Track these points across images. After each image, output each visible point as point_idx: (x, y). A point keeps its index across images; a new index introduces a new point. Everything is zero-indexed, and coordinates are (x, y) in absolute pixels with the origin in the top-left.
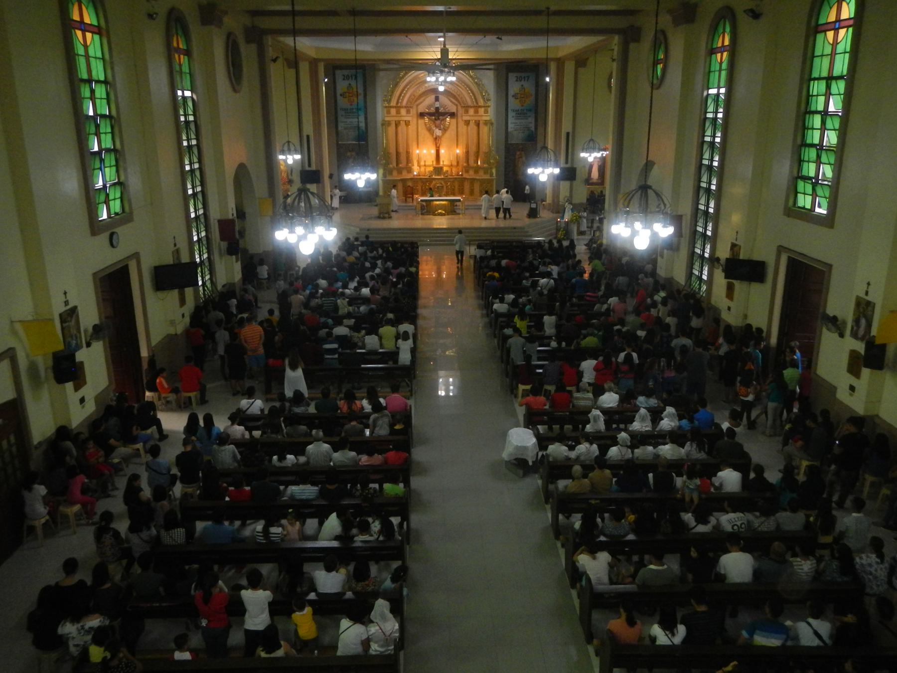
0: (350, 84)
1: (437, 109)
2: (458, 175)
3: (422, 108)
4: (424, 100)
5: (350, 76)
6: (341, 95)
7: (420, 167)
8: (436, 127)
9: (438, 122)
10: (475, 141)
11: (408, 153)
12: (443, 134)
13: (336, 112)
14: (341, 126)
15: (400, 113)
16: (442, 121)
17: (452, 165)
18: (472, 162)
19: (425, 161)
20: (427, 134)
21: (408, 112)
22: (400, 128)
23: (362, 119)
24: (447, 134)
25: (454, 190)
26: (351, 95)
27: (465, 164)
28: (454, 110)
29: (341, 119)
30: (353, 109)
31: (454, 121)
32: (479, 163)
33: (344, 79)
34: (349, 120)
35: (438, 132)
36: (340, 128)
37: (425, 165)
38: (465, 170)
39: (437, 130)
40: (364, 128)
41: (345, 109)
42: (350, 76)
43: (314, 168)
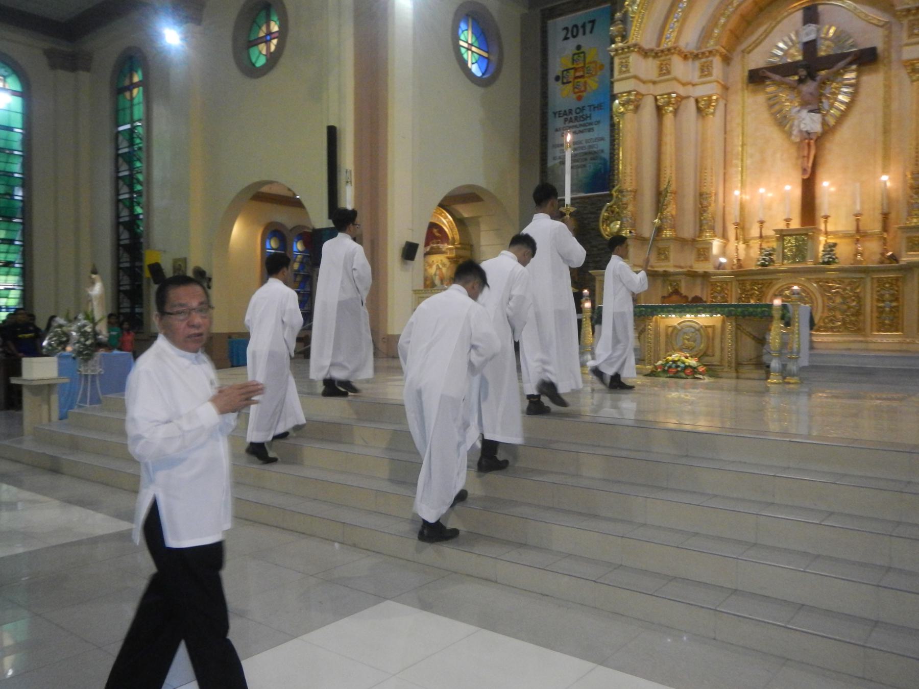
0: (579, 47)
1: (810, 47)
2: (882, 262)
3: (757, 60)
4: (767, 34)
5: (580, 24)
6: (557, 79)
7: (746, 242)
8: (804, 104)
9: (809, 87)
12: (828, 130)
13: (544, 125)
15: (669, 73)
16: (823, 83)
17: (858, 231)
19: (762, 222)
21: (705, 70)
22: (669, 119)
23: (602, 130)
24: (845, 132)
25: (858, 313)
26: (578, 74)
28: (874, 39)
30: (582, 109)
31: (873, 81)
33: (566, 38)
35: (811, 122)
36: (551, 163)
37: (761, 237)
38: (910, 239)
39: (804, 113)
40: (606, 155)
41: (565, 113)
42: (580, 24)
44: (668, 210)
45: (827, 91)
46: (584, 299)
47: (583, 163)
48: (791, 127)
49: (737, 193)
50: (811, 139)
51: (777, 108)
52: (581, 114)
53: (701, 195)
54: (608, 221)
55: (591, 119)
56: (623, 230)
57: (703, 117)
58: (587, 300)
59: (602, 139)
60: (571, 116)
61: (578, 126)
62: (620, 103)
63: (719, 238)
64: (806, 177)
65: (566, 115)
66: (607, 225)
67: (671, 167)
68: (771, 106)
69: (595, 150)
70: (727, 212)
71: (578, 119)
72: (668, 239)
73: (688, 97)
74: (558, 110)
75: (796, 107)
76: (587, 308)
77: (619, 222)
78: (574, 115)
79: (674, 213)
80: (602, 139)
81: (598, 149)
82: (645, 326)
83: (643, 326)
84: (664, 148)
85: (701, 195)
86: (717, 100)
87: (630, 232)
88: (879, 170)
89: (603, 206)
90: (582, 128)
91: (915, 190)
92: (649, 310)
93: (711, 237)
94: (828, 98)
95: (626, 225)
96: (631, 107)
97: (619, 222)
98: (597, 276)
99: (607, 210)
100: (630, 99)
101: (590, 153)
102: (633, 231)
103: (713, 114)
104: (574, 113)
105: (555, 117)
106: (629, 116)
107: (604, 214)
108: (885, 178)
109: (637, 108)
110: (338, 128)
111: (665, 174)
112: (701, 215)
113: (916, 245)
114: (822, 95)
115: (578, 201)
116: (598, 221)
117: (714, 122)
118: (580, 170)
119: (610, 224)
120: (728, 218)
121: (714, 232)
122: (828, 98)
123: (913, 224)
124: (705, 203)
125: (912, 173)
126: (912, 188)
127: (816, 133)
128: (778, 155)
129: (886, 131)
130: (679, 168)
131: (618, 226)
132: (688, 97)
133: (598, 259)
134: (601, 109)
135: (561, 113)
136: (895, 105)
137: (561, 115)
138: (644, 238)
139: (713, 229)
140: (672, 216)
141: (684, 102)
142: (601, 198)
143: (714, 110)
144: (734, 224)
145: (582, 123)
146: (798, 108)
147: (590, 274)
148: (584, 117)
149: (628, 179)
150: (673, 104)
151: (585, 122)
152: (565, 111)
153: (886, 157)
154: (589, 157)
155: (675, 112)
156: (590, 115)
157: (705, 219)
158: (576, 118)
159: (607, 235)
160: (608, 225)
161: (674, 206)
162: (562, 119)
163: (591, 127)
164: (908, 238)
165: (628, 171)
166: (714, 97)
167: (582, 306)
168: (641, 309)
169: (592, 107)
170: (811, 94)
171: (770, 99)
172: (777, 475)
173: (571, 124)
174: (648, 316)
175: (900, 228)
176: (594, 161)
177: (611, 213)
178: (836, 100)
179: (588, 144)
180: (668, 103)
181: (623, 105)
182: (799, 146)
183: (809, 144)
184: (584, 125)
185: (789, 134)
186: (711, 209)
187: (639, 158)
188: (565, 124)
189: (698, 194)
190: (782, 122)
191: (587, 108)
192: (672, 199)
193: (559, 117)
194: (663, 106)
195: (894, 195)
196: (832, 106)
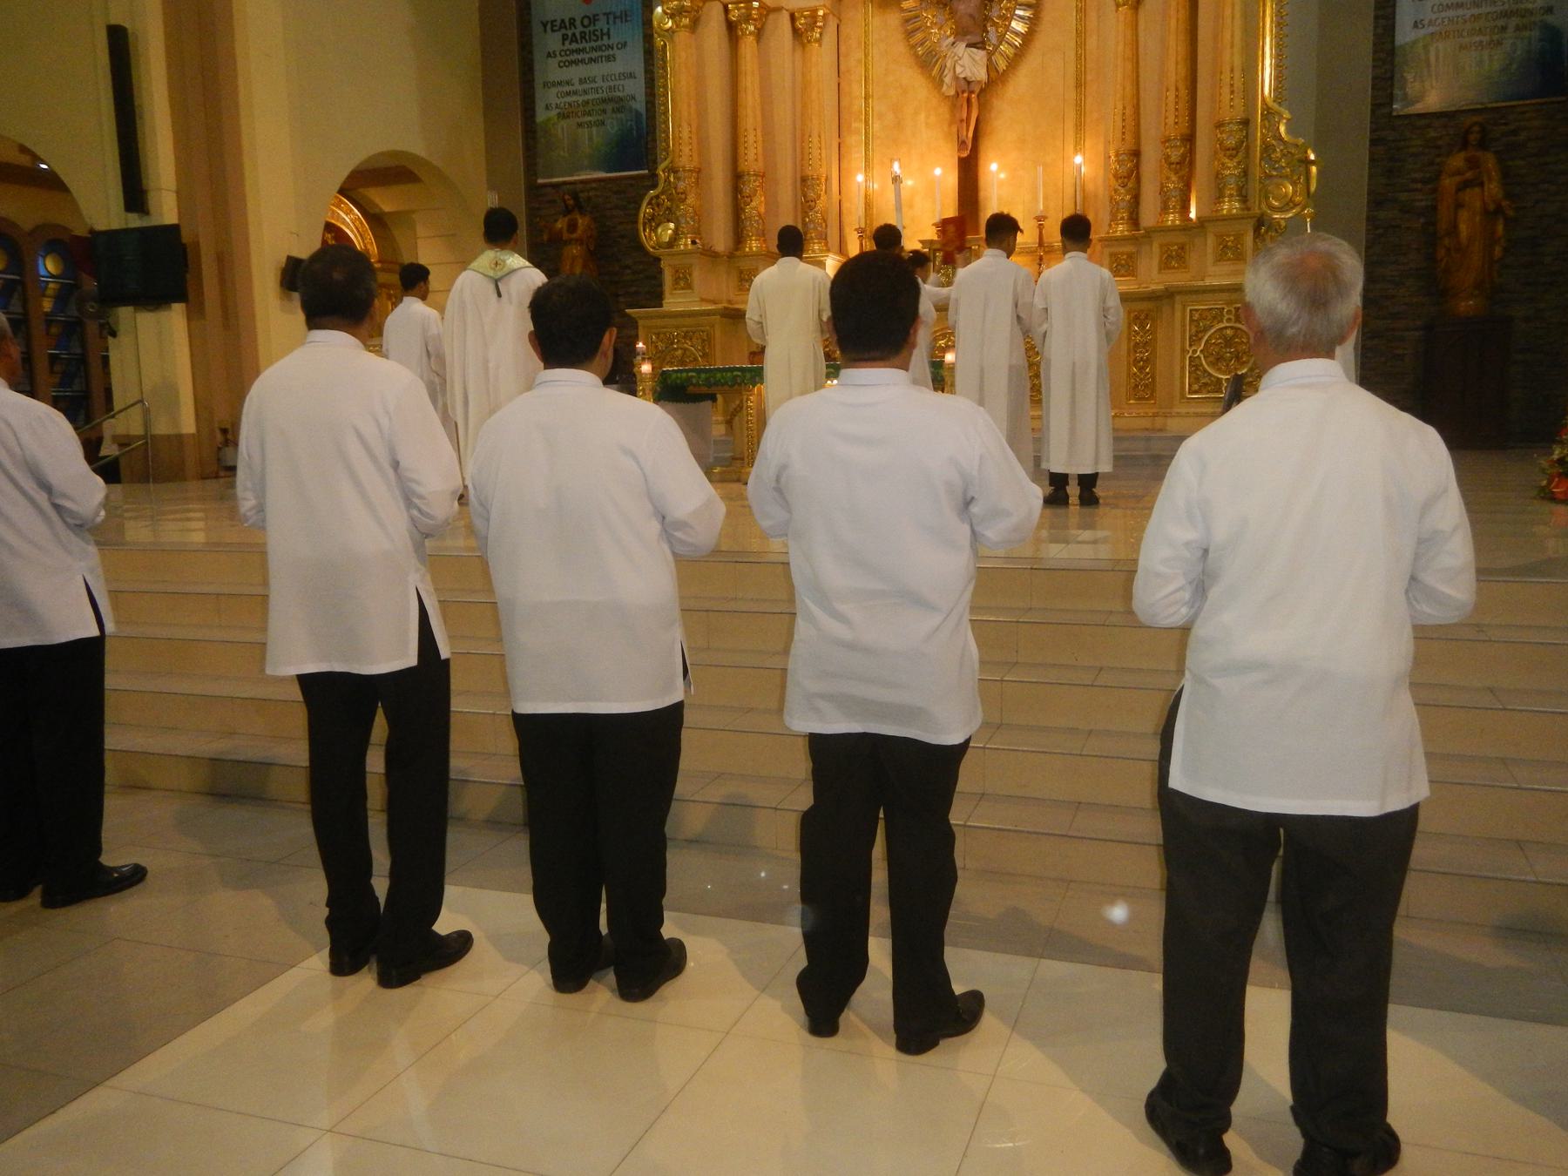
8: (960, 33)
10: (1175, 70)
11: (804, 181)
12: (996, 79)
13: (526, 46)
14: (548, 104)
17: (1041, 243)
18: (1149, 217)
20: (919, 86)
22: (748, 46)
23: (630, 61)
24: (1021, 83)
27: (1121, 229)
29: (549, 70)
30: (593, 19)
32: (1193, 215)
34: (575, 73)
35: (970, 64)
36: (541, 116)
38: (1114, 257)
39: (961, 47)
40: (640, 105)
41: (563, 24)
43: (166, 209)
44: (754, 204)
45: (994, 13)
46: (639, 358)
47: (600, 118)
48: (943, 69)
49: (860, 178)
50: (972, 92)
51: (919, 36)
52: (592, 28)
53: (804, 180)
54: (654, 222)
55: (609, 38)
56: (681, 238)
57: (803, 46)
58: (643, 359)
59: (632, 76)
60: (573, 30)
61: (588, 50)
62: (664, 11)
63: (835, 253)
64: (965, 154)
65: (566, 27)
66: (651, 230)
67: (755, 130)
68: (909, 34)
69: (620, 94)
70: (844, 211)
71: (587, 37)
72: (753, 255)
73: (778, 9)
74: (550, 17)
75: (948, 37)
76: (646, 374)
77: (672, 225)
78: (580, 28)
79: (762, 210)
80: (632, 76)
81: (625, 94)
82: (742, 401)
83: (737, 402)
84: (742, 95)
85: (804, 180)
86: (824, 16)
87: (694, 242)
88: (1070, 148)
89: (646, 194)
90: (594, 55)
91: (1120, 181)
92: (748, 375)
93: (821, 251)
94: (995, 24)
95: (685, 231)
96: (686, 21)
97: (672, 225)
98: (641, 318)
99: (650, 203)
100: (683, 6)
101: (611, 100)
102: (697, 241)
103: (819, 41)
104: (578, 23)
105: (545, 31)
106: (682, 37)
107: (645, 210)
108: (1078, 159)
109: (695, 24)
110: (130, 31)
111: (745, 142)
112: (805, 214)
113: (1123, 266)
114: (987, 19)
115: (594, 185)
116: (636, 222)
117: (822, 55)
118: (594, 129)
119: (658, 225)
120: (846, 219)
121: (826, 244)
122: (995, 24)
123: (1118, 234)
124: (811, 195)
125: (1117, 155)
126: (1116, 177)
127: (979, 82)
128: (922, 116)
129: (1080, 84)
130: (768, 133)
131: (670, 232)
132: (778, 9)
133: (634, 289)
134: (626, 21)
135: (555, 23)
136: (1092, 43)
137: (555, 28)
138: (714, 252)
139: (826, 239)
140: (759, 215)
141: (771, 17)
142: (633, 182)
143: (821, 34)
144: (856, 230)
145: (593, 44)
146: (951, 39)
147: (628, 316)
148: (598, 33)
149: (686, 150)
150: (755, 20)
151: (599, 43)
152: (563, 21)
153: (1079, 126)
154: (609, 107)
155: (759, 34)
156: (609, 29)
157: (811, 221)
158: (583, 37)
159: (654, 248)
160: (654, 230)
161: (763, 198)
162: (558, 36)
163: (611, 52)
164: (1111, 255)
165: (685, 134)
166: (821, 13)
167: (635, 370)
168: (735, 373)
169: (611, 17)
170: (971, 16)
171: (907, 21)
172: (1021, 620)
173: (574, 46)
174: (746, 384)
175: (1101, 240)
176: (619, 116)
177: (656, 208)
178: (1007, 28)
179: (608, 84)
180: (748, 18)
181: (672, 16)
182: (953, 101)
183: (969, 100)
184: (599, 48)
185: (938, 83)
186: (820, 205)
187: (702, 114)
188: (563, 44)
189: (799, 180)
190: (928, 62)
191: (603, 19)
192: (758, 187)
193: (553, 31)
194: (739, 22)
195: (1090, 187)
196: (1001, 39)
